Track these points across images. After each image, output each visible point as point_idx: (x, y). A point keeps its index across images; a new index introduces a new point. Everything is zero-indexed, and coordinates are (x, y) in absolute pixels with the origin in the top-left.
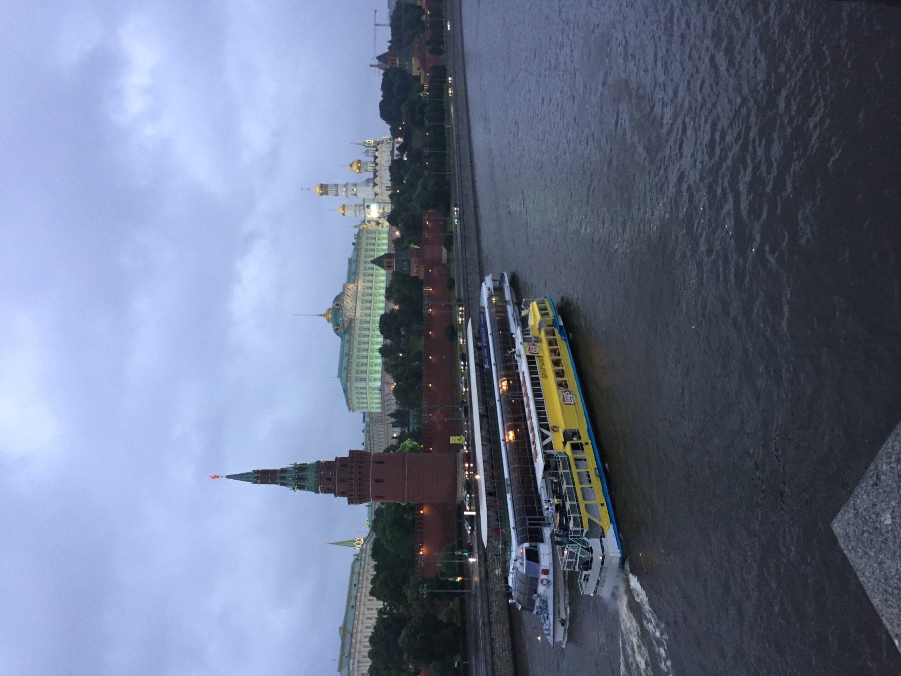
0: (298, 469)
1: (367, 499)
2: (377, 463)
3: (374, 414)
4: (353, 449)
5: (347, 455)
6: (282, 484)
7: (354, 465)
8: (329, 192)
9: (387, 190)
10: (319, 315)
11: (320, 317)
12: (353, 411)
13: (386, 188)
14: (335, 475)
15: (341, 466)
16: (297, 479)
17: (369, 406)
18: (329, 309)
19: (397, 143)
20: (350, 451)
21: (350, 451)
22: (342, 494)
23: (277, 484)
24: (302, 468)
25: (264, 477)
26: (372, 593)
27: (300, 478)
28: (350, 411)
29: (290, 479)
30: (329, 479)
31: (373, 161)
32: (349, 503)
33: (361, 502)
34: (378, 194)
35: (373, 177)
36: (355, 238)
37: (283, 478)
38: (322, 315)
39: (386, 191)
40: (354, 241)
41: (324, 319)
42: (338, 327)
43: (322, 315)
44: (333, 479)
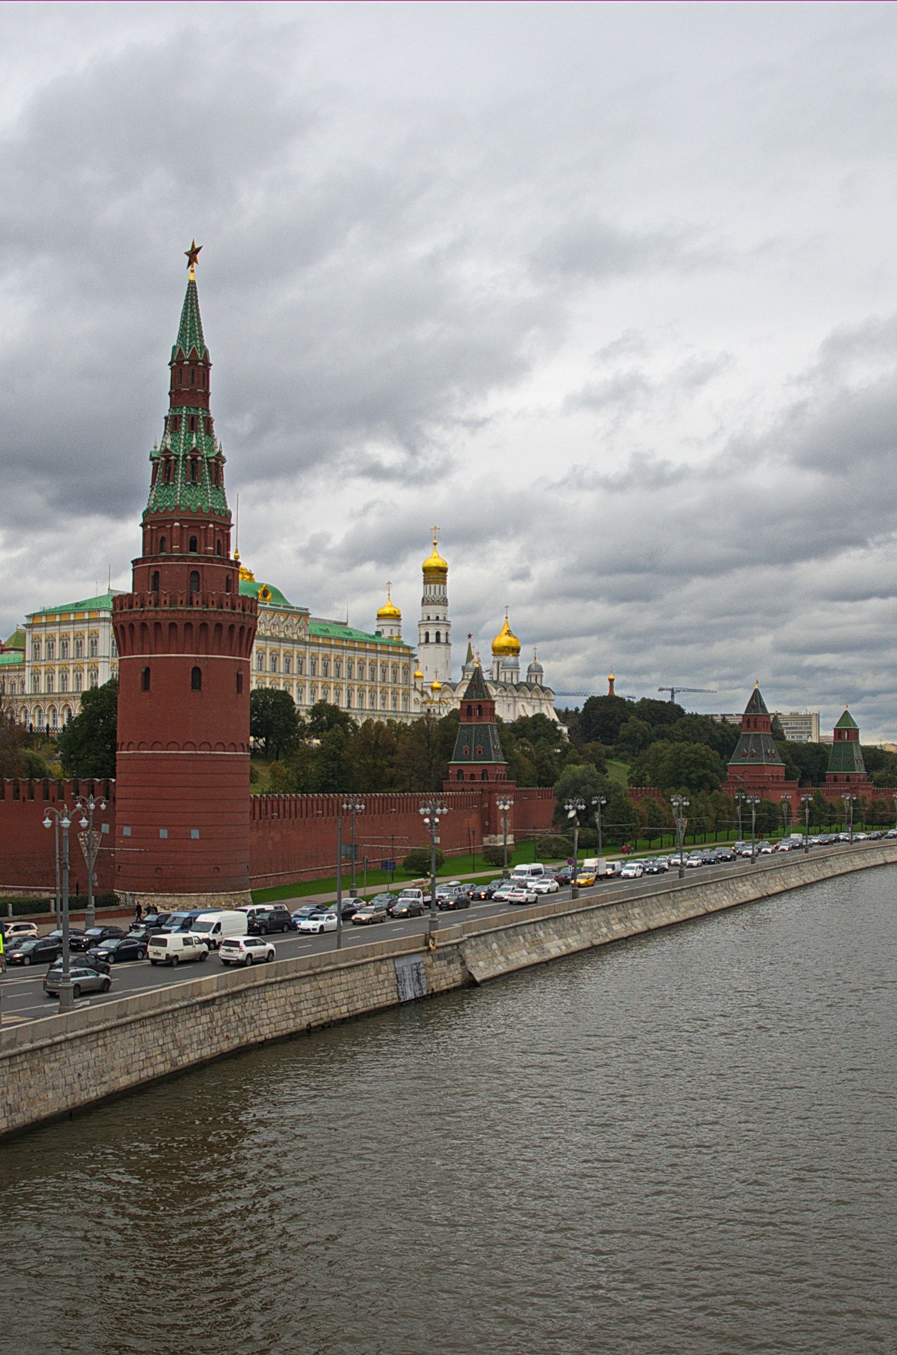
0: (217, 465)
7: (237, 611)
8: (433, 586)
18: (251, 575)
23: (174, 405)
28: (27, 617)
30: (193, 547)
34: (454, 690)
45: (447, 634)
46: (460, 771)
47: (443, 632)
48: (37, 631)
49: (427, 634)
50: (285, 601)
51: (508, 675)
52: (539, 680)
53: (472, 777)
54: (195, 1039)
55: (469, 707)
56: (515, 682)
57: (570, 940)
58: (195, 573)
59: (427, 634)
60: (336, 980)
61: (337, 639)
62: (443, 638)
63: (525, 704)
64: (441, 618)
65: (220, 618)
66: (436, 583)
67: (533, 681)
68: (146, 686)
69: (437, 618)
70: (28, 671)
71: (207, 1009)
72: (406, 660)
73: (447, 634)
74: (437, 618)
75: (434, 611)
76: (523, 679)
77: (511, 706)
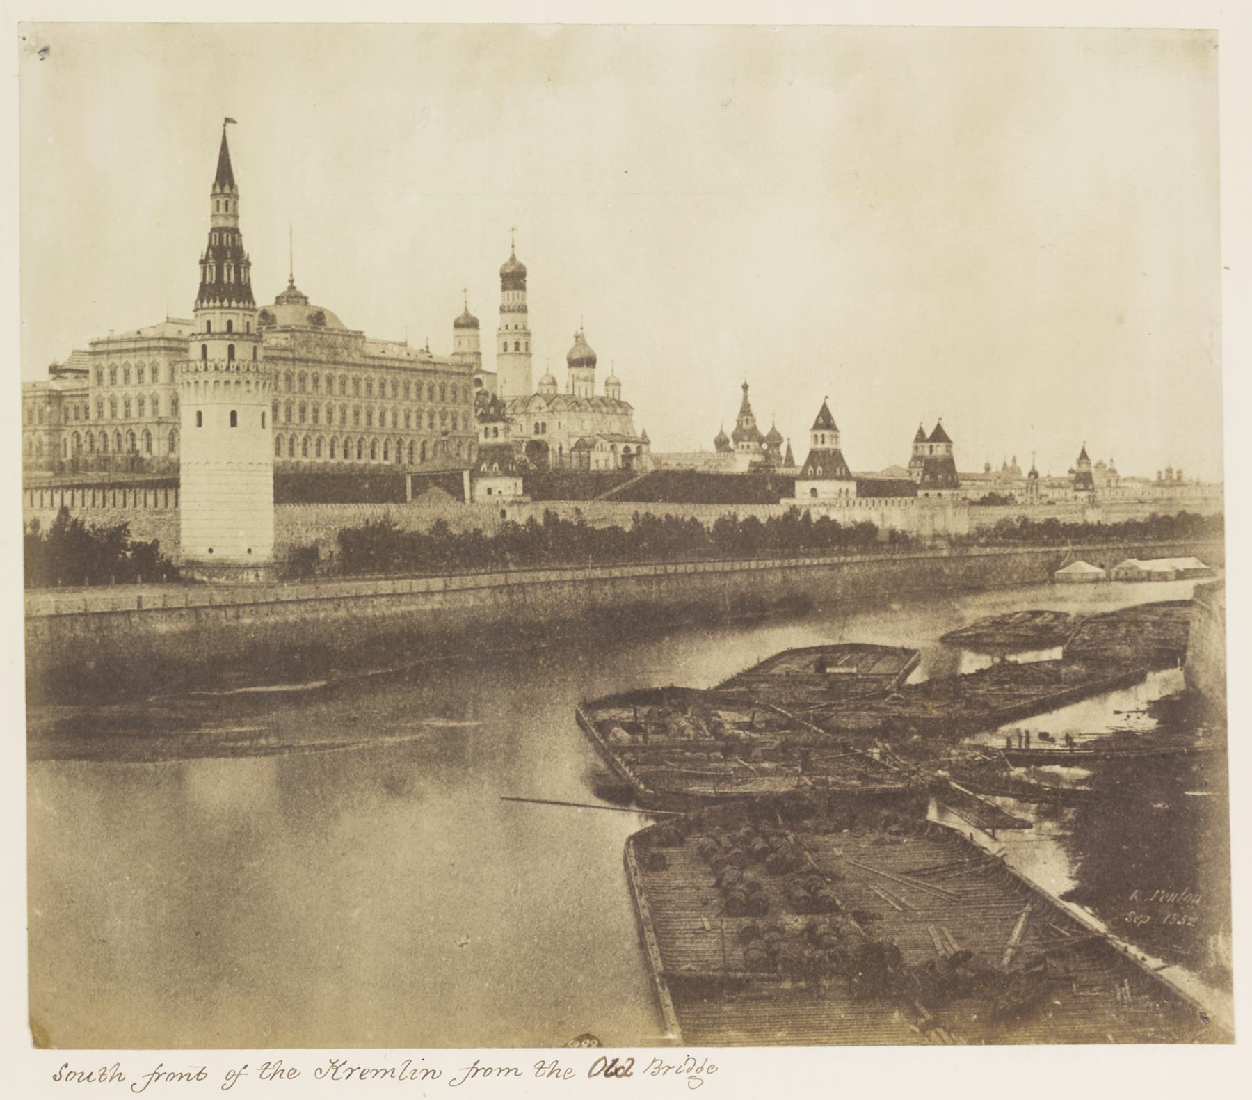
11: (288, 278)
13: (540, 422)
38: (292, 281)
43: (292, 281)
45: (527, 343)
47: (522, 341)
49: (505, 344)
52: (616, 393)
59: (505, 344)
62: (522, 349)
64: (520, 327)
69: (516, 327)
73: (527, 343)
74: (516, 327)
76: (600, 391)
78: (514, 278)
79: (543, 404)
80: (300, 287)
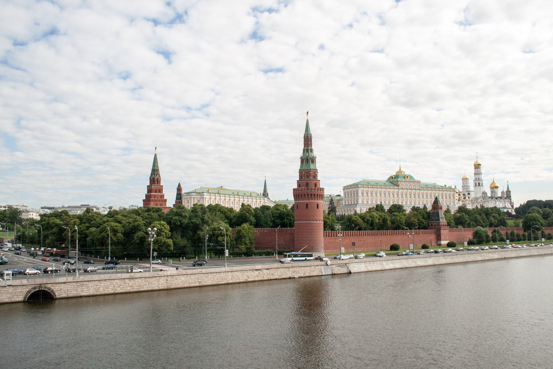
1: (296, 199)
2: (317, 204)
3: (342, 201)
4: (325, 190)
5: (321, 187)
6: (304, 150)
8: (477, 169)
9: (481, 205)
10: (400, 167)
12: (343, 189)
13: (482, 204)
14: (310, 180)
15: (315, 183)
16: (307, 158)
17: (347, 199)
19: (511, 211)
20: (324, 188)
21: (324, 188)
22: (299, 185)
24: (313, 161)
25: (308, 140)
26: (243, 205)
27: (307, 160)
29: (307, 154)
31: (499, 196)
32: (294, 190)
33: (294, 195)
35: (488, 196)
36: (449, 187)
37: (307, 150)
38: (400, 168)
39: (480, 205)
40: (447, 186)
41: (398, 170)
42: (394, 178)
43: (400, 168)
44: (307, 179)
46: (432, 224)
47: (481, 182)
48: (346, 190)
49: (476, 183)
50: (414, 179)
51: (494, 195)
53: (435, 225)
54: (253, 276)
55: (434, 207)
56: (496, 197)
57: (396, 265)
58: (307, 183)
59: (476, 183)
60: (300, 269)
61: (430, 188)
62: (481, 184)
63: (499, 203)
65: (311, 193)
66: (477, 168)
67: (503, 196)
68: (297, 208)
69: (479, 179)
70: (344, 200)
71: (257, 271)
72: (453, 192)
73: (482, 183)
74: (479, 179)
75: (478, 176)
76: (500, 195)
77: (495, 204)
78: (477, 166)
79: (482, 199)
80: (402, 169)
